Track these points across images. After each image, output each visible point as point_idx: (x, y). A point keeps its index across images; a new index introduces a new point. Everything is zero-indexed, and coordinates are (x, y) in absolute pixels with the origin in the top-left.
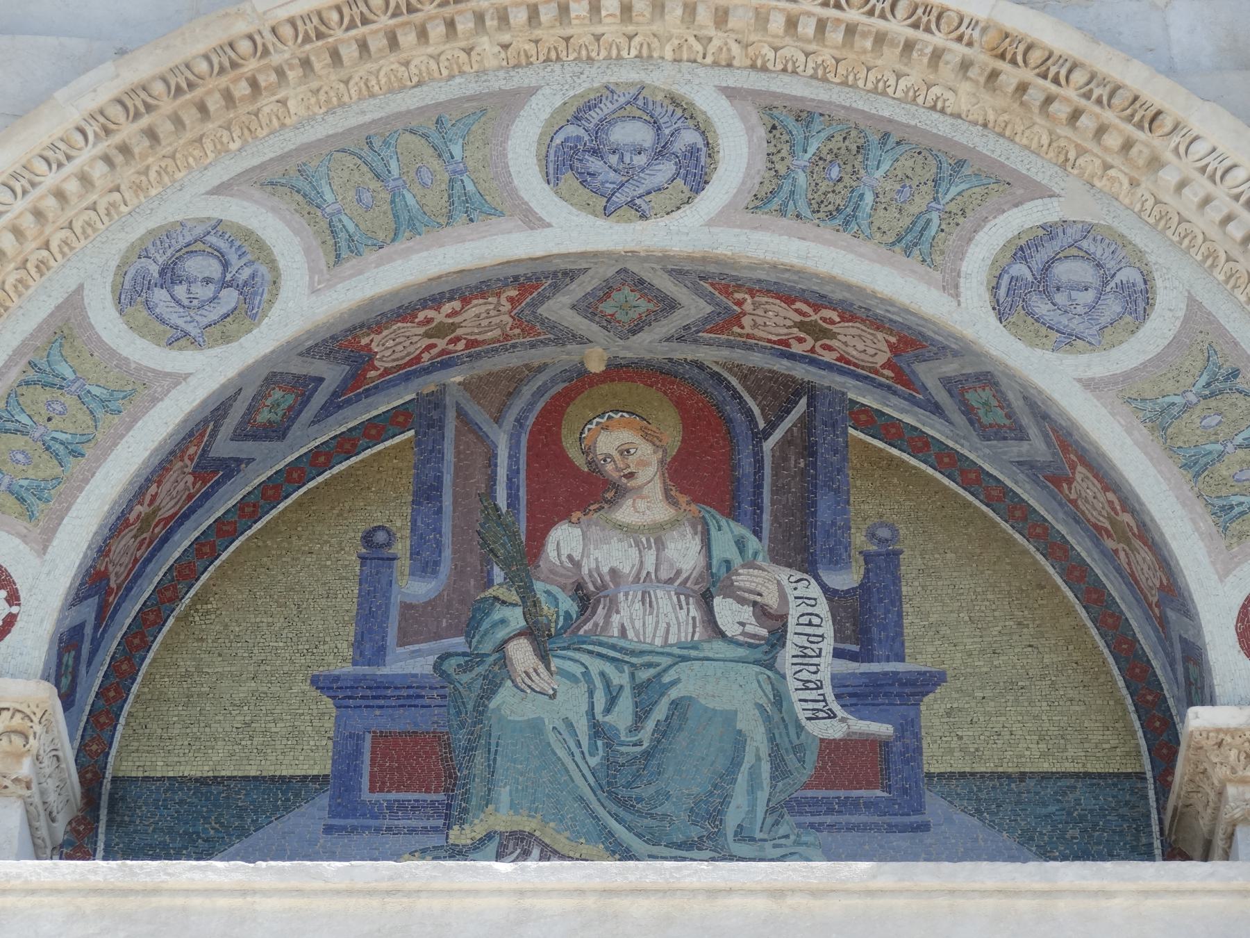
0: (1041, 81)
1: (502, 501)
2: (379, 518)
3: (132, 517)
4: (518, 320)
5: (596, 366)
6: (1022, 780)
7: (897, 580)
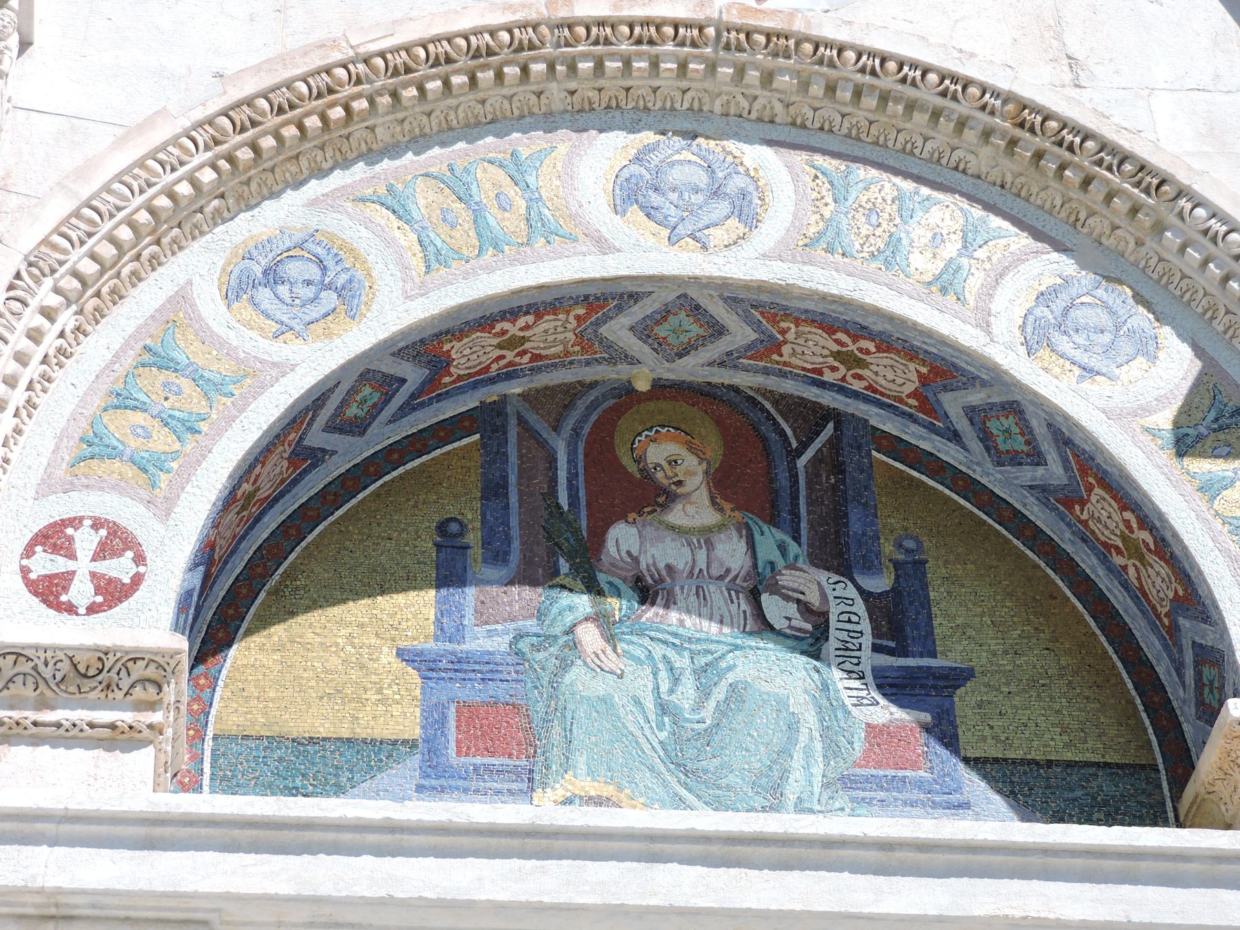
0: (1056, 149)
1: (563, 500)
2: (452, 511)
3: (240, 493)
4: (580, 336)
5: (642, 386)
6: (1049, 767)
7: (925, 586)
